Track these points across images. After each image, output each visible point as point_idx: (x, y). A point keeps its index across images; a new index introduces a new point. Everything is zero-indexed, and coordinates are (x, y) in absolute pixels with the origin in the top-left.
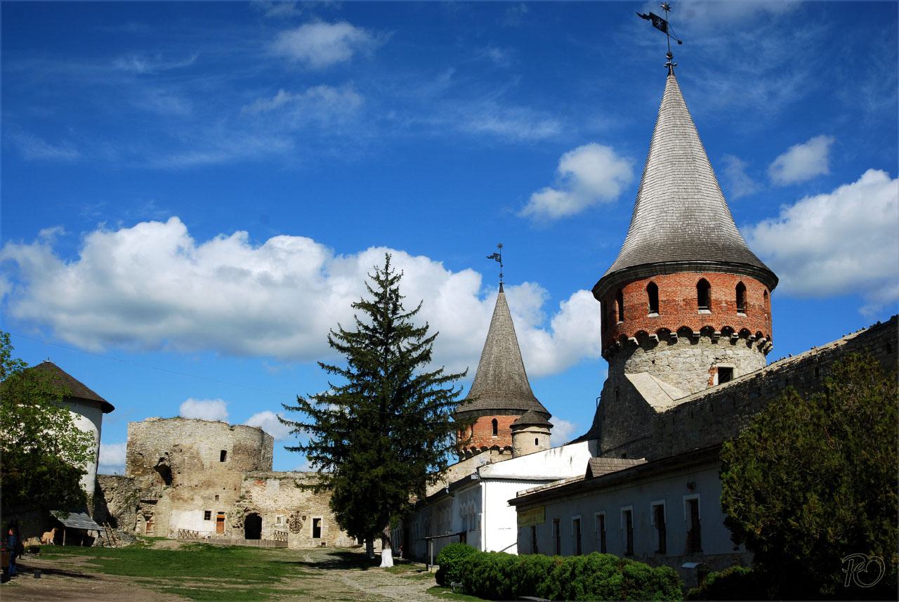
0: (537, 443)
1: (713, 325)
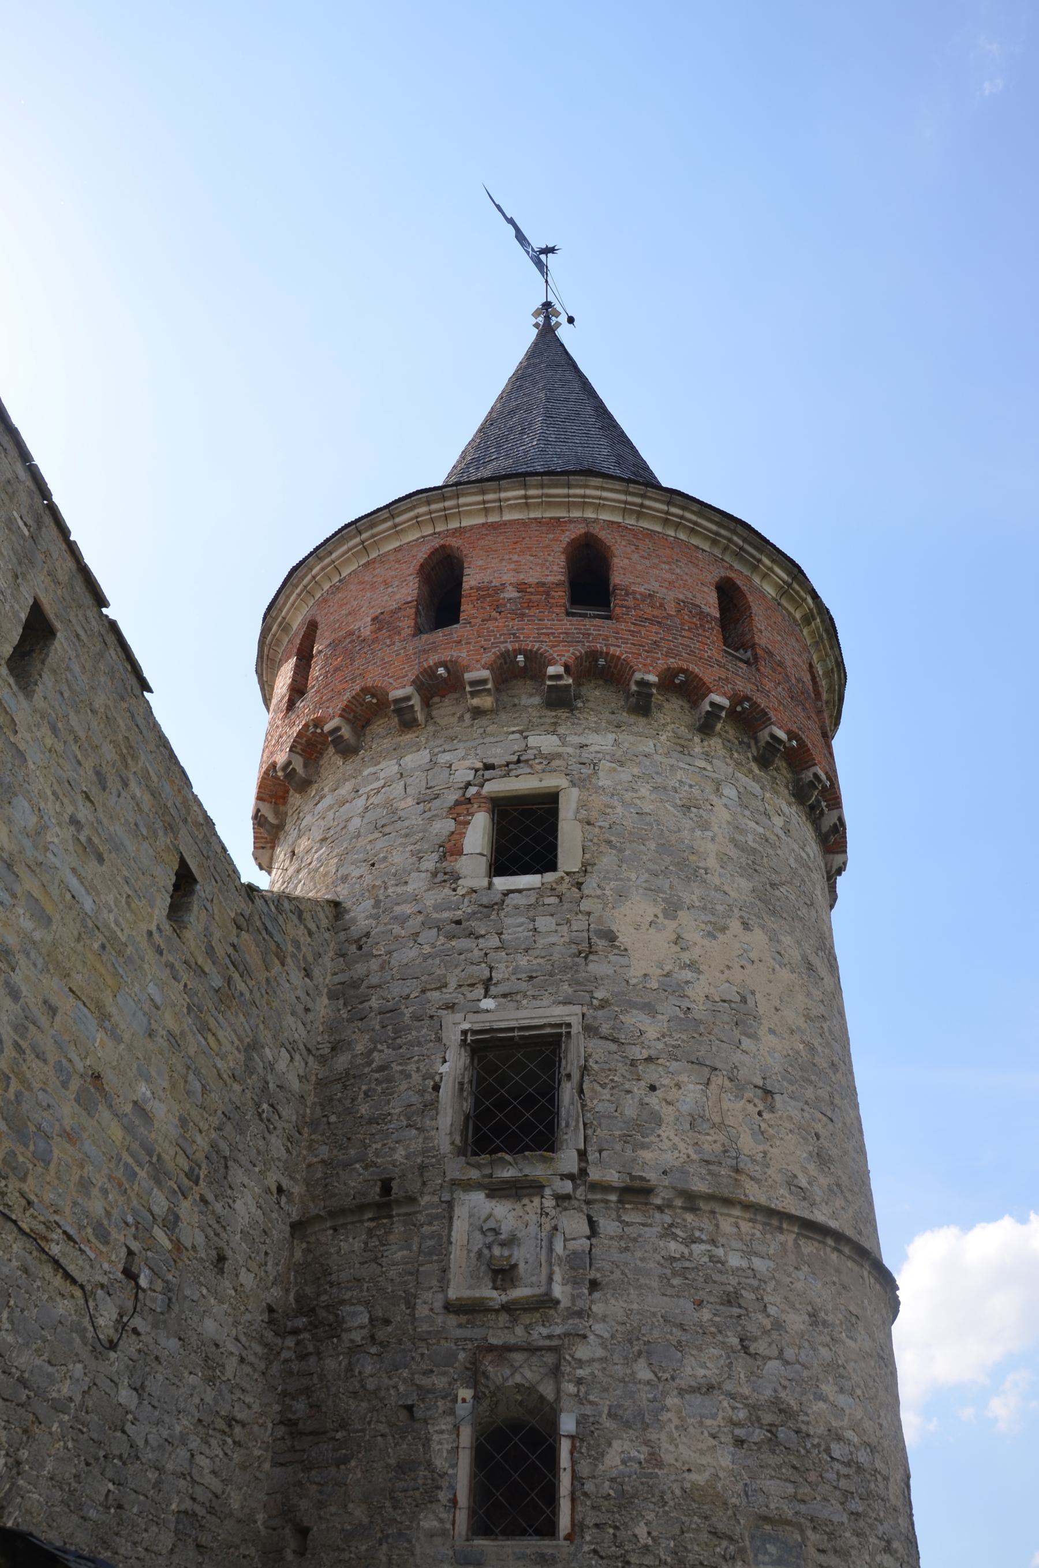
1: (462, 654)
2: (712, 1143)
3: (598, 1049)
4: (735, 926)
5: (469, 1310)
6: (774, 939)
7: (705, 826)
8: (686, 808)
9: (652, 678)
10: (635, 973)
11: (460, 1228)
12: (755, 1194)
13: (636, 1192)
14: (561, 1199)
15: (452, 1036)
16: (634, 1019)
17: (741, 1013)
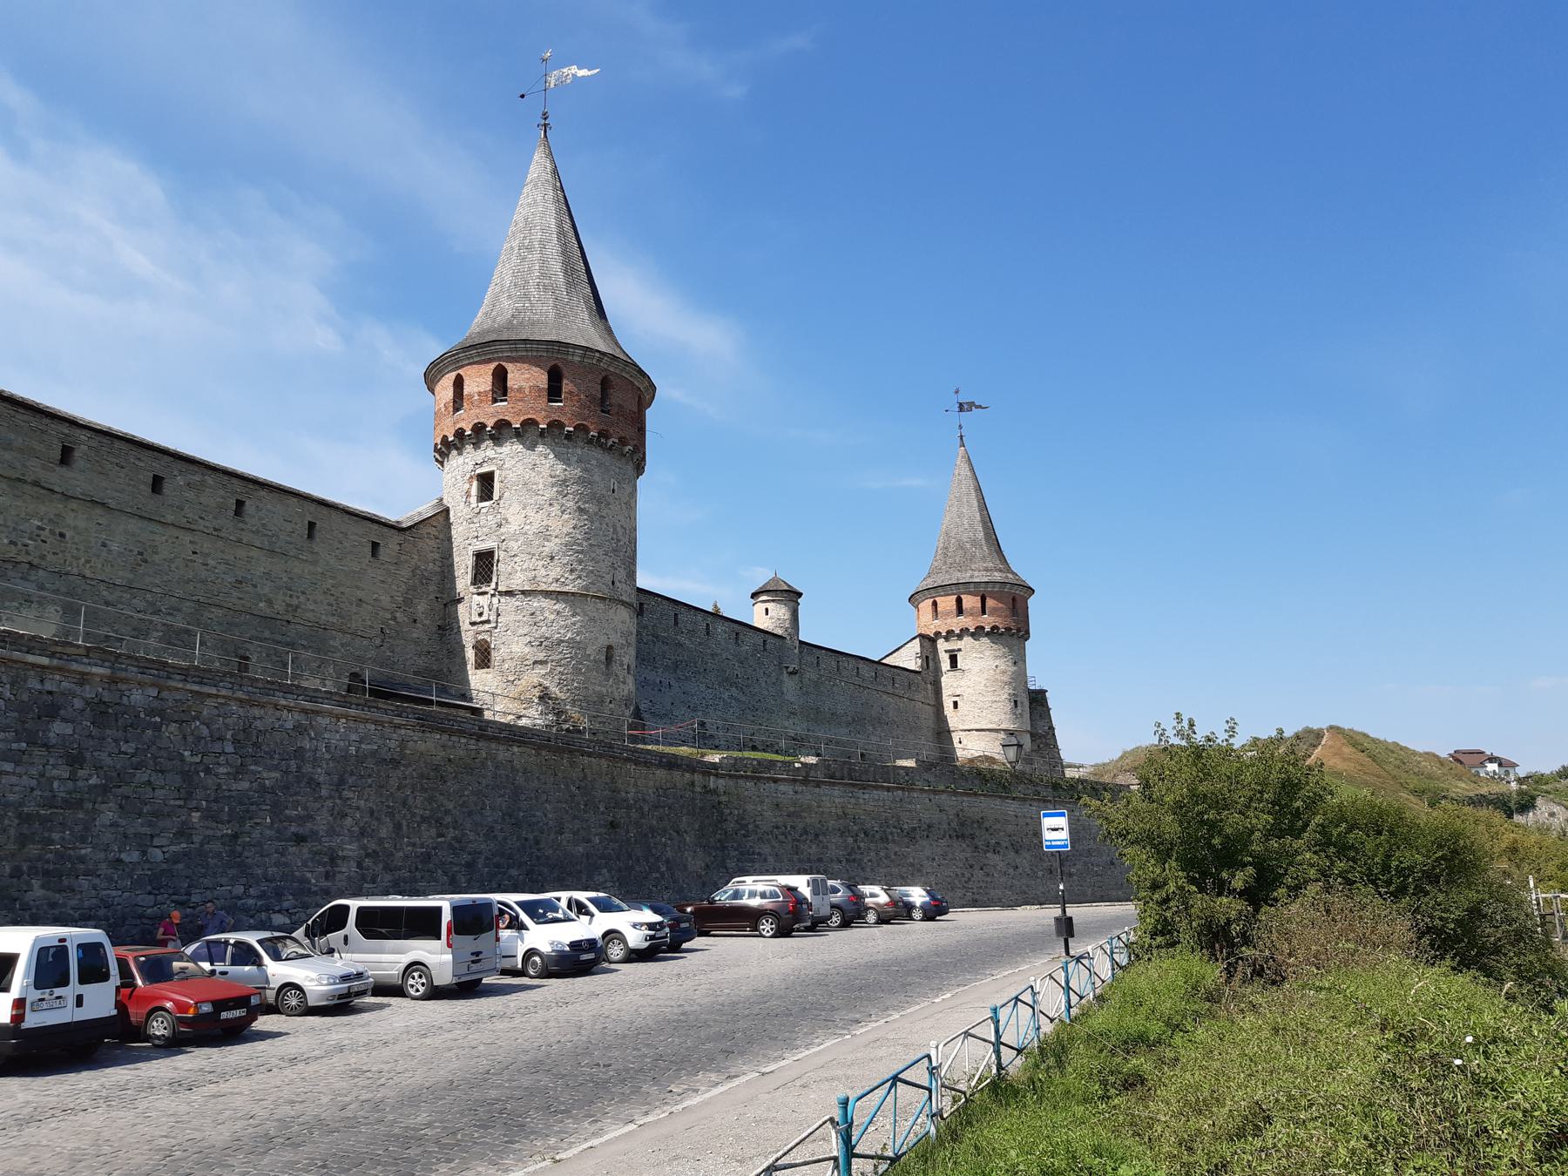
5: (473, 624)
12: (543, 587)
13: (510, 593)
16: (512, 544)
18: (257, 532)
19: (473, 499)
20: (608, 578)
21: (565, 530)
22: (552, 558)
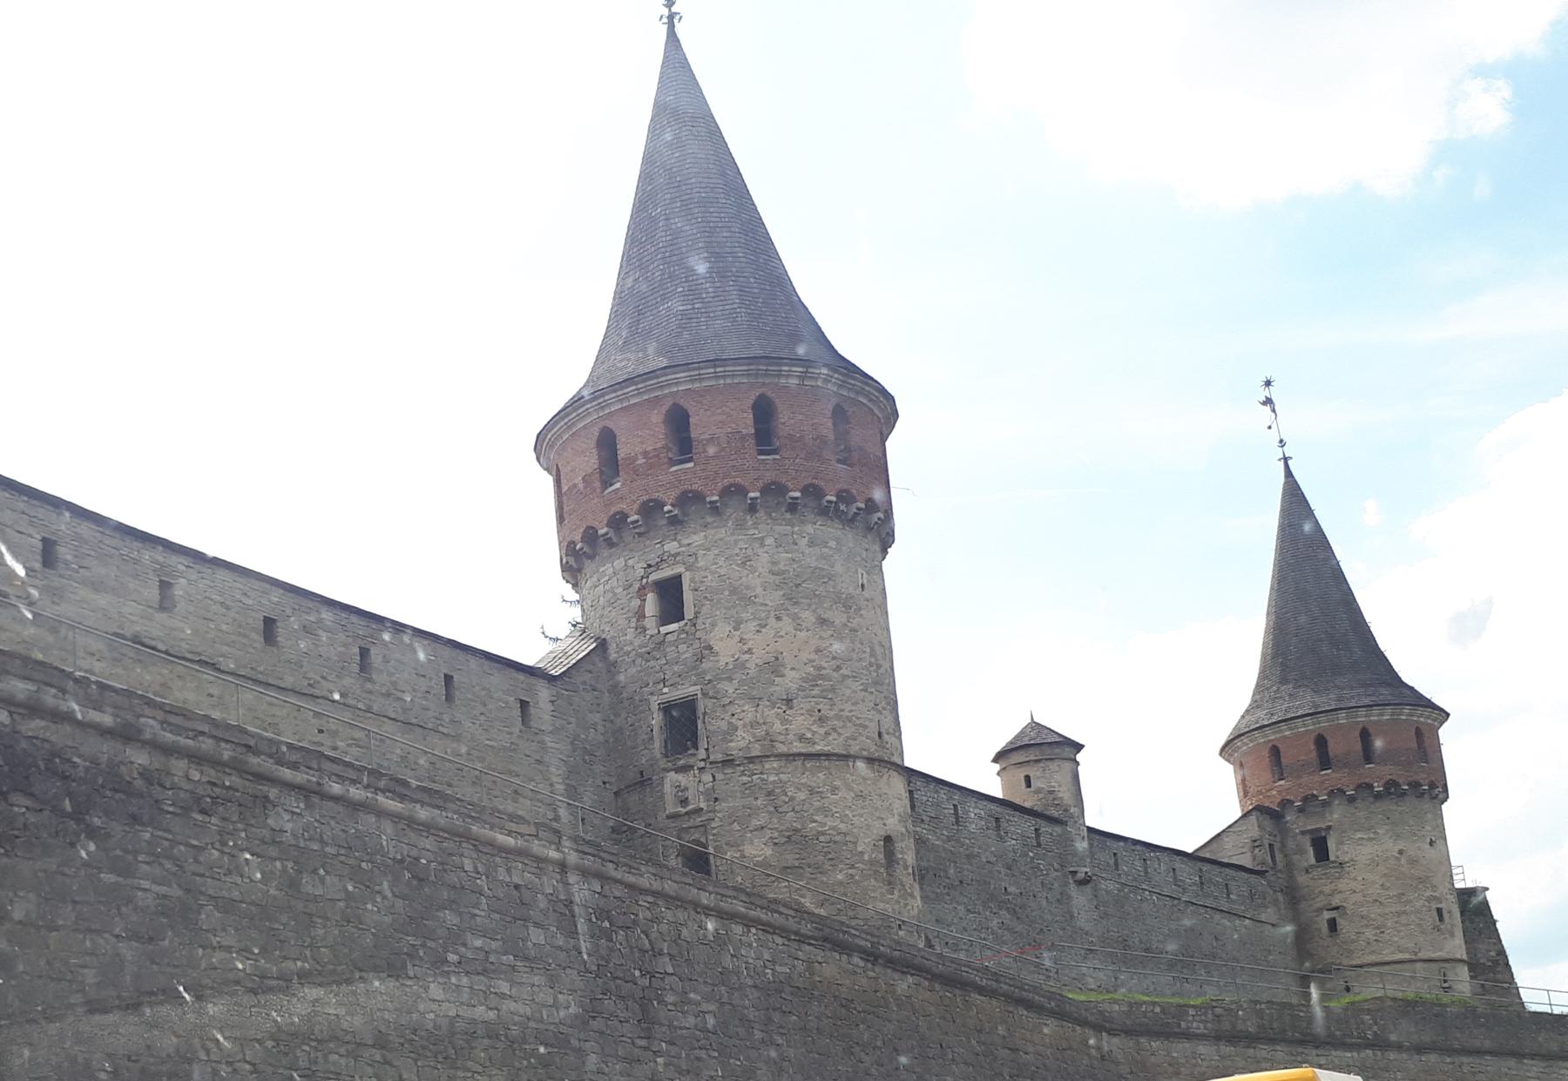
0: (1029, 785)
1: (623, 506)
2: (760, 732)
3: (710, 703)
4: (772, 621)
6: (795, 618)
7: (753, 570)
8: (744, 563)
9: (716, 498)
10: (722, 663)
11: (668, 788)
12: (782, 749)
13: (728, 762)
14: (700, 769)
15: (655, 707)
17: (774, 667)
18: (388, 695)
19: (650, 624)
20: (873, 727)
21: (805, 656)
22: (789, 702)
